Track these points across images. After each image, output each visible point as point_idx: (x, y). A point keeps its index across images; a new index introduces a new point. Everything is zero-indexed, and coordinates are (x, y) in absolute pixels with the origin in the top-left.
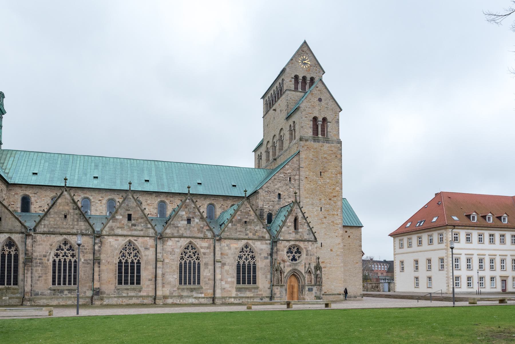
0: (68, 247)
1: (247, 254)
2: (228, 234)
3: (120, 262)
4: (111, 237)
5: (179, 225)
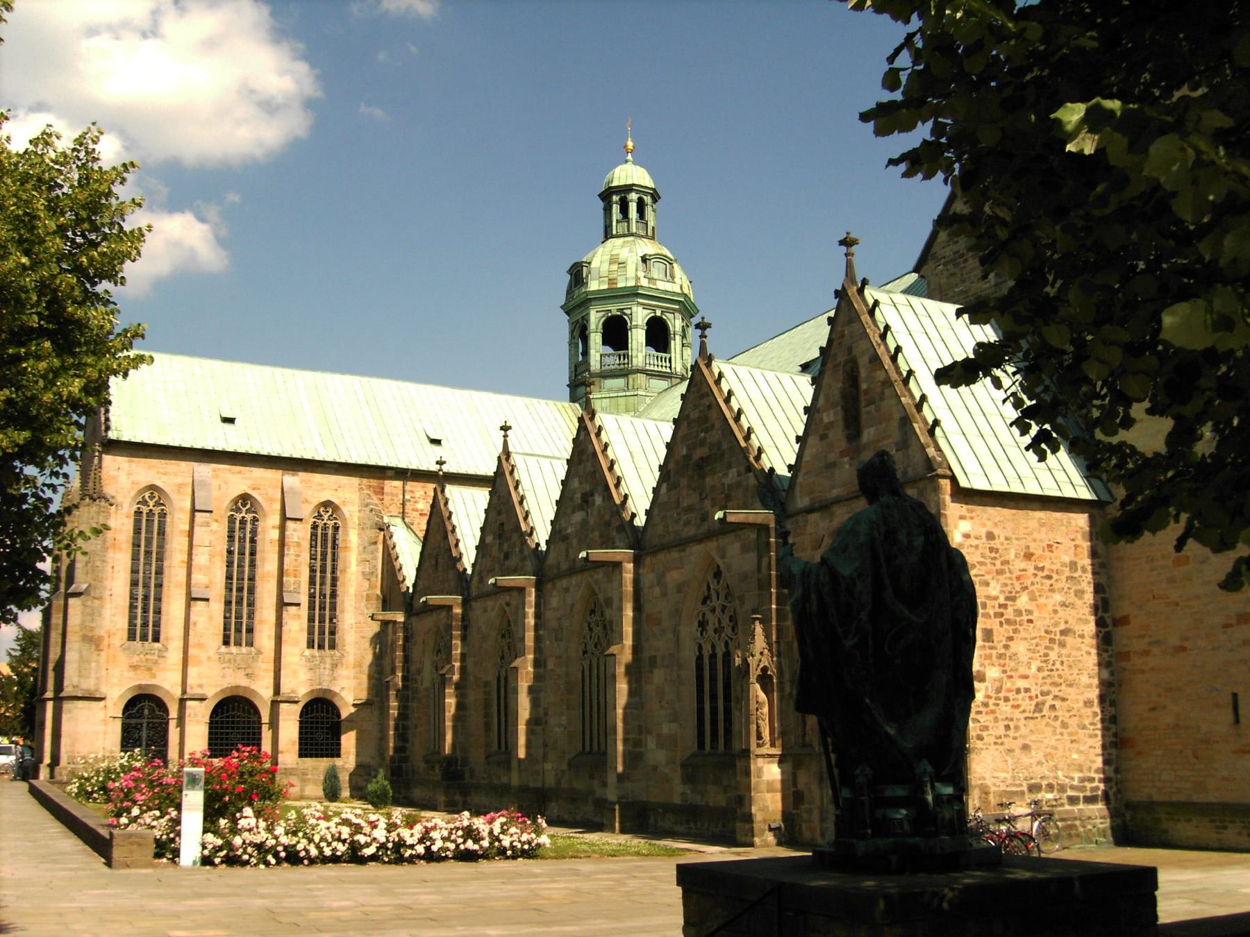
5: (569, 530)
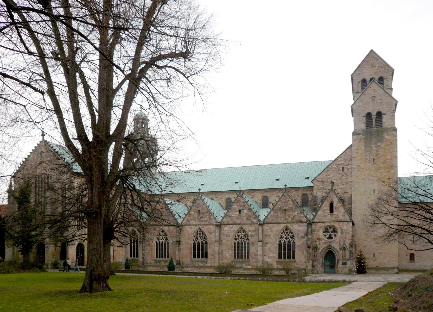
0: (164, 233)
1: (287, 234)
2: (270, 219)
3: (194, 243)
4: (187, 226)
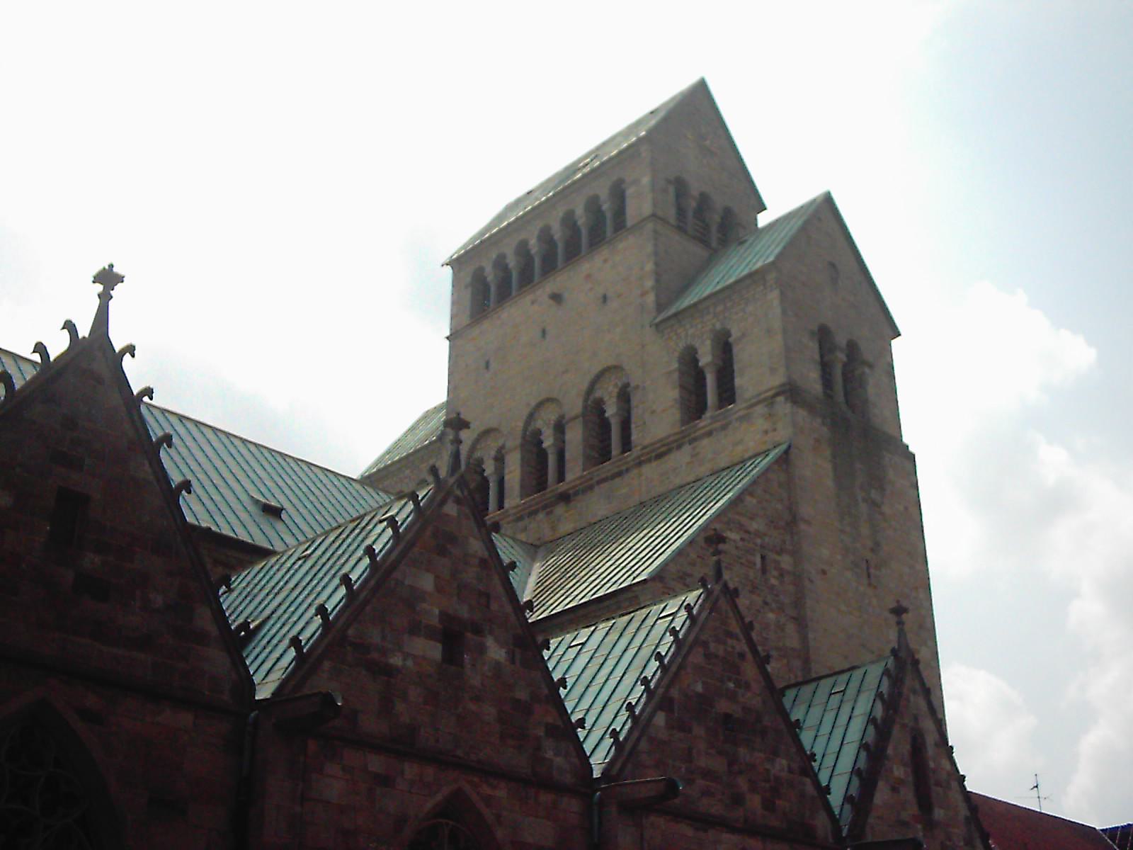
5: (396, 660)
